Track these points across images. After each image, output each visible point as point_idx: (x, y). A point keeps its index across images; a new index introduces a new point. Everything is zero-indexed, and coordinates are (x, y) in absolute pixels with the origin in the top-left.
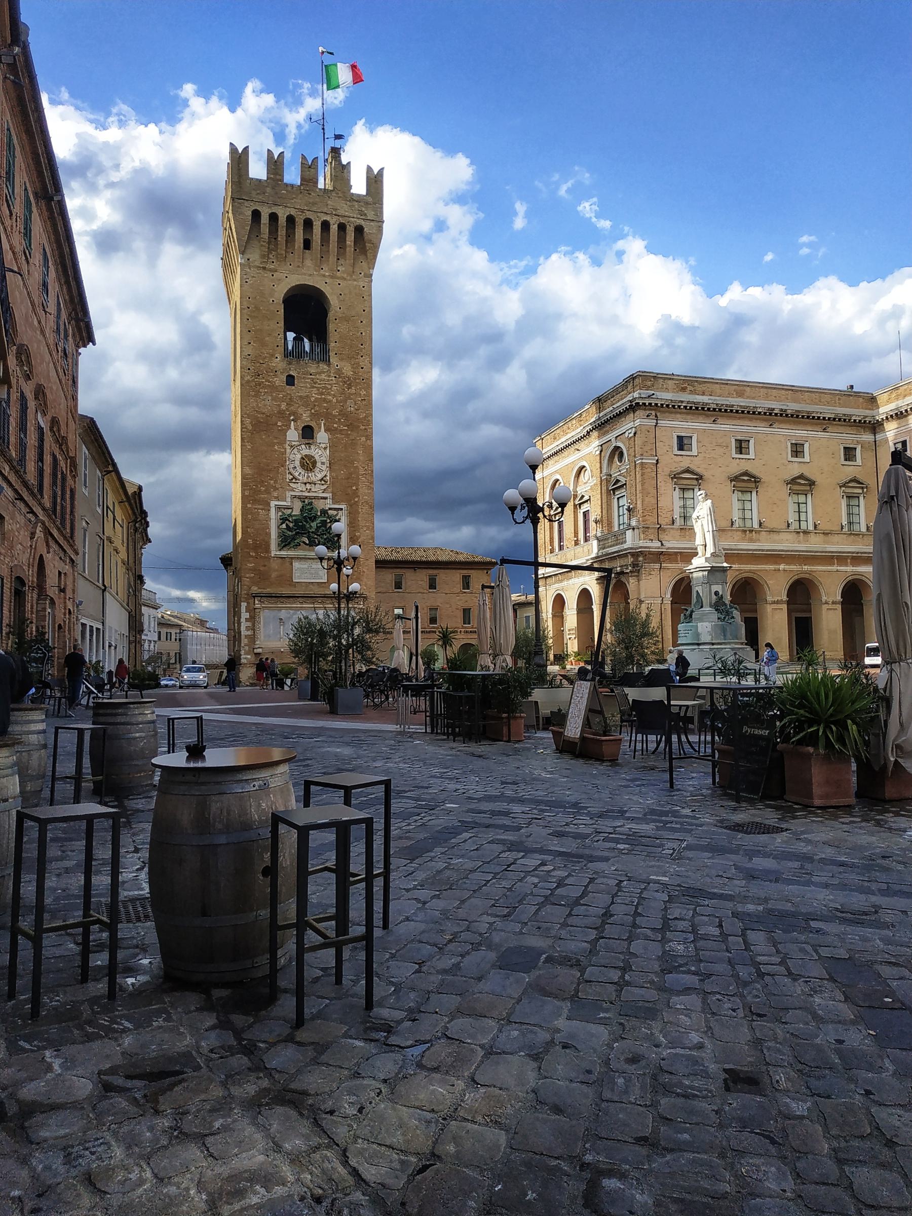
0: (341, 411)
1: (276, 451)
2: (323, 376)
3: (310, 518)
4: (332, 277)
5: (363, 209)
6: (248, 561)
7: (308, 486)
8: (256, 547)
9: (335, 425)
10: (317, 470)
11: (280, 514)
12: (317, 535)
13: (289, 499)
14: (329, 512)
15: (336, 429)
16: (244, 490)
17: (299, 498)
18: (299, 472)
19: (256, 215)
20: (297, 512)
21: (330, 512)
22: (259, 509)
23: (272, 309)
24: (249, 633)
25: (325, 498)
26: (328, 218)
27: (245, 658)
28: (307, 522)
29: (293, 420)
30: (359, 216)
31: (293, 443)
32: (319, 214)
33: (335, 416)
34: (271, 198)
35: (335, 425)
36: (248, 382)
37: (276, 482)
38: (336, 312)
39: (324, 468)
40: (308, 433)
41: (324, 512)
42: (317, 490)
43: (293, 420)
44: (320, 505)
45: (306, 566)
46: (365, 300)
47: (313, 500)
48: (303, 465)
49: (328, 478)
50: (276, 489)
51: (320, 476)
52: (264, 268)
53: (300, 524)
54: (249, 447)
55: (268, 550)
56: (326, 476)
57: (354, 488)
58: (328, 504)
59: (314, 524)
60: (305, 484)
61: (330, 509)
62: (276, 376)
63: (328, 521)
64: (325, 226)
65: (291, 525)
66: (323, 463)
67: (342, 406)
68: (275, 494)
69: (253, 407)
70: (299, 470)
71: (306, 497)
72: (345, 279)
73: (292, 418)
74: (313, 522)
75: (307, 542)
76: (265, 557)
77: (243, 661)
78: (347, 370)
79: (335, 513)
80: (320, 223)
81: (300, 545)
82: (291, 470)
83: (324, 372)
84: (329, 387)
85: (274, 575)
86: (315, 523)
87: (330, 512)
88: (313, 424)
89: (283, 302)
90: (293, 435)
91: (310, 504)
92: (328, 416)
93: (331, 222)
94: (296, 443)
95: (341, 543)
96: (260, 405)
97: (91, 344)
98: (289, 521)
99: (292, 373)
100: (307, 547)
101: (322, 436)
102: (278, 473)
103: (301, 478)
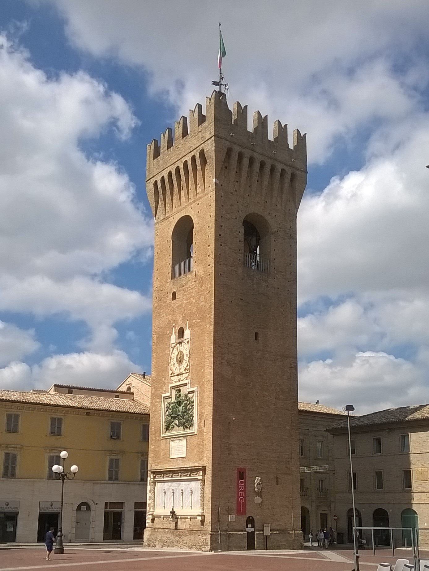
15: (194, 323)
25: (186, 384)
29: (174, 326)
40: (181, 333)
42: (184, 379)
44: (184, 391)
45: (176, 444)
47: (180, 388)
53: (175, 409)
58: (188, 388)
59: (180, 408)
60: (178, 375)
61: (189, 393)
62: (167, 296)
63: (188, 403)
67: (198, 303)
69: (157, 326)
70: (177, 365)
71: (178, 386)
74: (180, 405)
75: (178, 424)
78: (201, 273)
86: (181, 406)
88: (183, 326)
90: (174, 339)
91: (180, 391)
101: (187, 333)
103: (176, 371)
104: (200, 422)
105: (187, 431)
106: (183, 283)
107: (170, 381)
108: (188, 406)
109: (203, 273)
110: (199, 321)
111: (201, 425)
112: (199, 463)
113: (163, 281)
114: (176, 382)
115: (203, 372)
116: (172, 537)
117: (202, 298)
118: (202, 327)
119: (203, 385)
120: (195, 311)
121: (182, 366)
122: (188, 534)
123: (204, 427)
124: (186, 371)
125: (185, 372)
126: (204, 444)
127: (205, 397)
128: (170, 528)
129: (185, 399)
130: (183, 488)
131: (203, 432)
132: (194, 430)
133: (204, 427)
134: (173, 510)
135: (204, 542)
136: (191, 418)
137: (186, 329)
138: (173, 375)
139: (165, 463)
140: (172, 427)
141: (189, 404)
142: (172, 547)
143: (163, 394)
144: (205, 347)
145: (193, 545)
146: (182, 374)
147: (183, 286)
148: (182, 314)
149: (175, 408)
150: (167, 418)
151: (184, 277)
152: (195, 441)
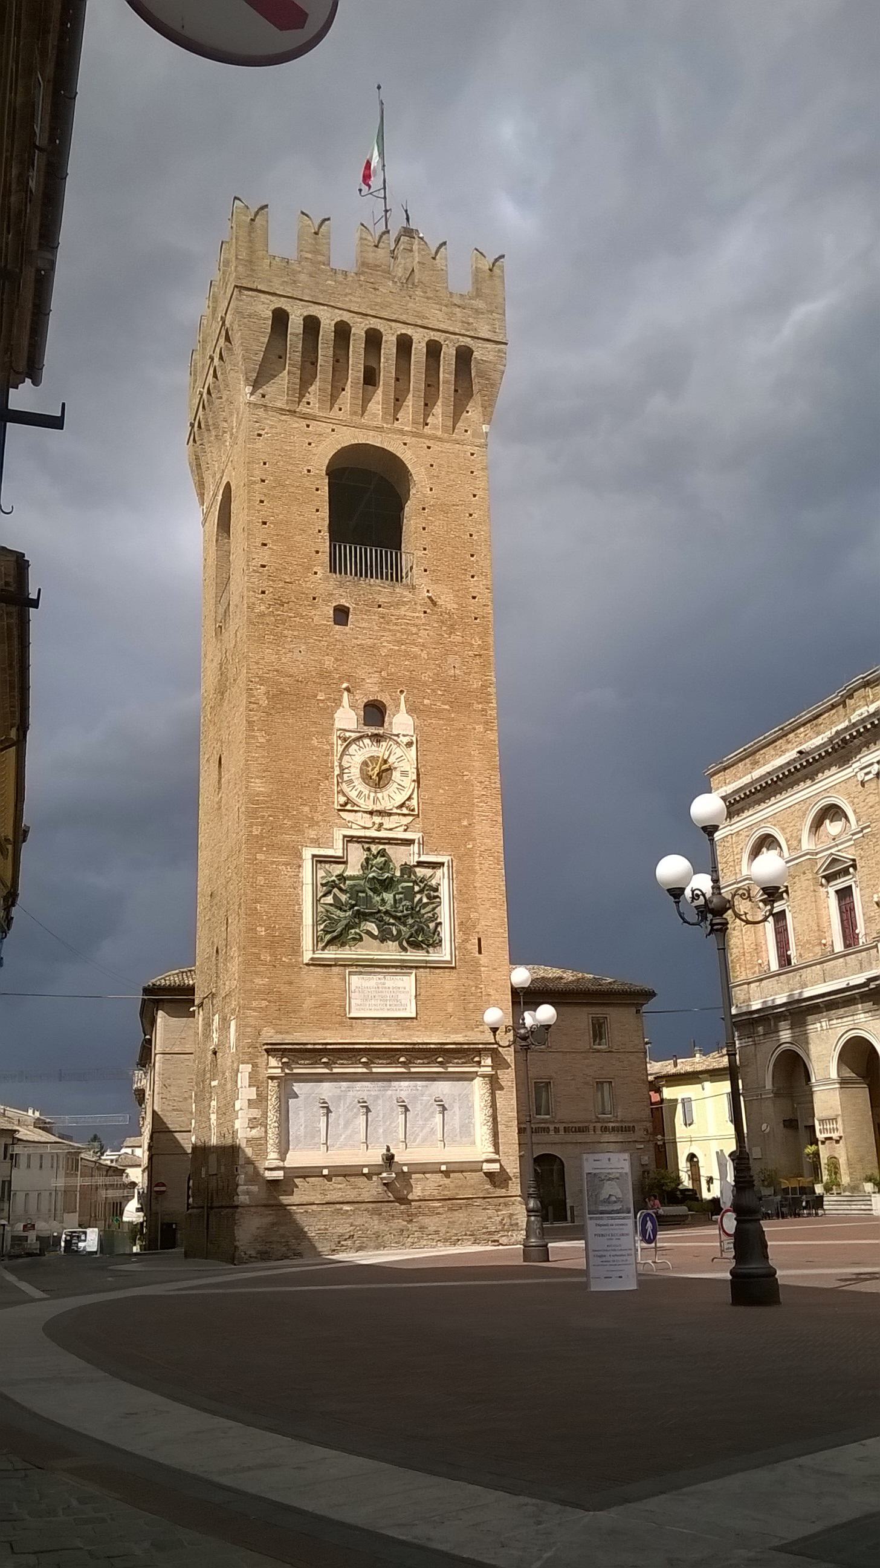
0: (437, 675)
1: (314, 748)
2: (403, 611)
3: (382, 882)
4: (415, 435)
5: (471, 320)
6: (257, 973)
7: (377, 820)
8: (272, 944)
9: (426, 702)
10: (392, 788)
11: (321, 873)
12: (395, 918)
13: (339, 844)
14: (417, 870)
15: (429, 707)
16: (251, 825)
17: (357, 840)
18: (358, 790)
19: (280, 318)
20: (353, 869)
21: (421, 872)
22: (278, 863)
23: (307, 484)
24: (254, 1133)
25: (409, 842)
26: (409, 331)
27: (248, 1193)
28: (375, 891)
29: (348, 690)
30: (463, 332)
31: (348, 734)
32: (393, 324)
33: (425, 684)
34: (306, 291)
35: (426, 702)
36: (262, 615)
37: (314, 809)
38: (424, 496)
39: (409, 783)
40: (375, 713)
41: (407, 869)
42: (394, 827)
43: (348, 690)
46: (476, 478)
47: (386, 847)
48: (366, 778)
49: (414, 803)
50: (313, 823)
51: (400, 799)
52: (293, 412)
54: (263, 740)
55: (296, 949)
56: (409, 799)
57: (465, 823)
59: (388, 897)
60: (371, 813)
61: (420, 864)
63: (417, 888)
64: (404, 345)
65: (344, 898)
66: (404, 774)
68: (312, 834)
71: (374, 840)
72: (440, 440)
73: (345, 685)
75: (376, 933)
76: (291, 966)
77: (243, 1199)
78: (447, 601)
79: (428, 872)
80: (394, 338)
81: (361, 939)
82: (344, 786)
83: (405, 603)
84: (414, 630)
85: (308, 1002)
87: (421, 872)
88: (385, 698)
89: (327, 474)
90: (347, 718)
91: (382, 853)
92: (412, 685)
93: (415, 339)
94: (354, 735)
95: (442, 935)
96: (284, 660)
97: (28, 381)
98: (341, 889)
99: (343, 602)
100: (376, 943)
101: (401, 722)
102: (317, 790)
103: (361, 802)
104: (466, 941)
105: (413, 955)
106: (382, 600)
107: (337, 821)
108: (418, 896)
109: (456, 606)
110: (447, 707)
111: (469, 946)
112: (466, 1036)
113: (296, 563)
114: (365, 828)
115: (466, 827)
116: (376, 1222)
117: (451, 659)
118: (457, 725)
119: (470, 854)
120: (431, 680)
121: (386, 793)
122: (441, 1210)
123: (480, 952)
124: (405, 811)
125: (399, 811)
126: (481, 992)
127: (478, 885)
128: (359, 1199)
129: (402, 876)
130: (403, 1095)
131: (477, 964)
132: (444, 953)
133: (480, 952)
134: (388, 1149)
135: (504, 1222)
136: (432, 925)
137: (398, 711)
138: (349, 807)
139: (323, 1029)
140: (354, 939)
141: (420, 892)
142: (377, 1248)
143: (306, 846)
144: (470, 771)
145: (466, 1235)
146: (390, 815)
147: (380, 606)
148: (379, 670)
149: (363, 892)
150: (327, 911)
151: (385, 588)
152: (448, 982)
